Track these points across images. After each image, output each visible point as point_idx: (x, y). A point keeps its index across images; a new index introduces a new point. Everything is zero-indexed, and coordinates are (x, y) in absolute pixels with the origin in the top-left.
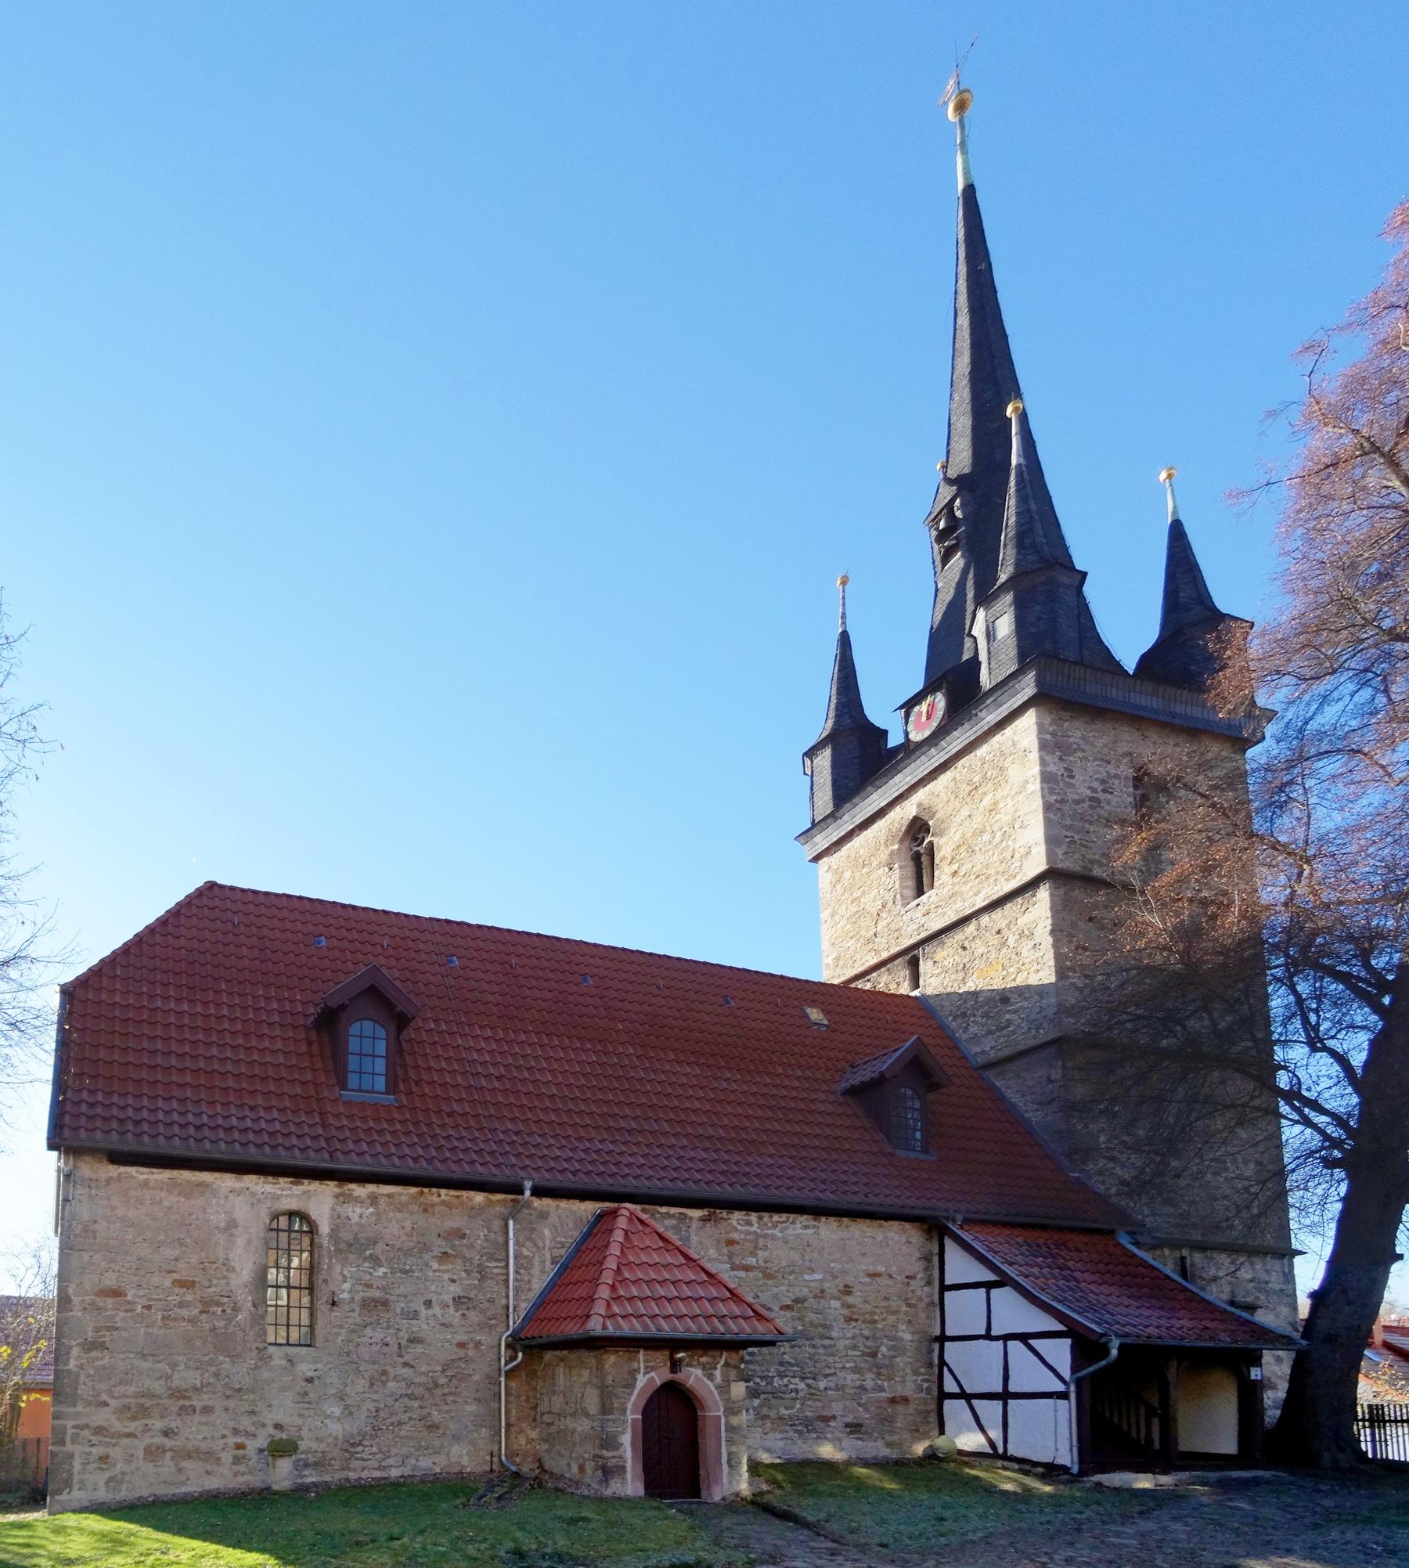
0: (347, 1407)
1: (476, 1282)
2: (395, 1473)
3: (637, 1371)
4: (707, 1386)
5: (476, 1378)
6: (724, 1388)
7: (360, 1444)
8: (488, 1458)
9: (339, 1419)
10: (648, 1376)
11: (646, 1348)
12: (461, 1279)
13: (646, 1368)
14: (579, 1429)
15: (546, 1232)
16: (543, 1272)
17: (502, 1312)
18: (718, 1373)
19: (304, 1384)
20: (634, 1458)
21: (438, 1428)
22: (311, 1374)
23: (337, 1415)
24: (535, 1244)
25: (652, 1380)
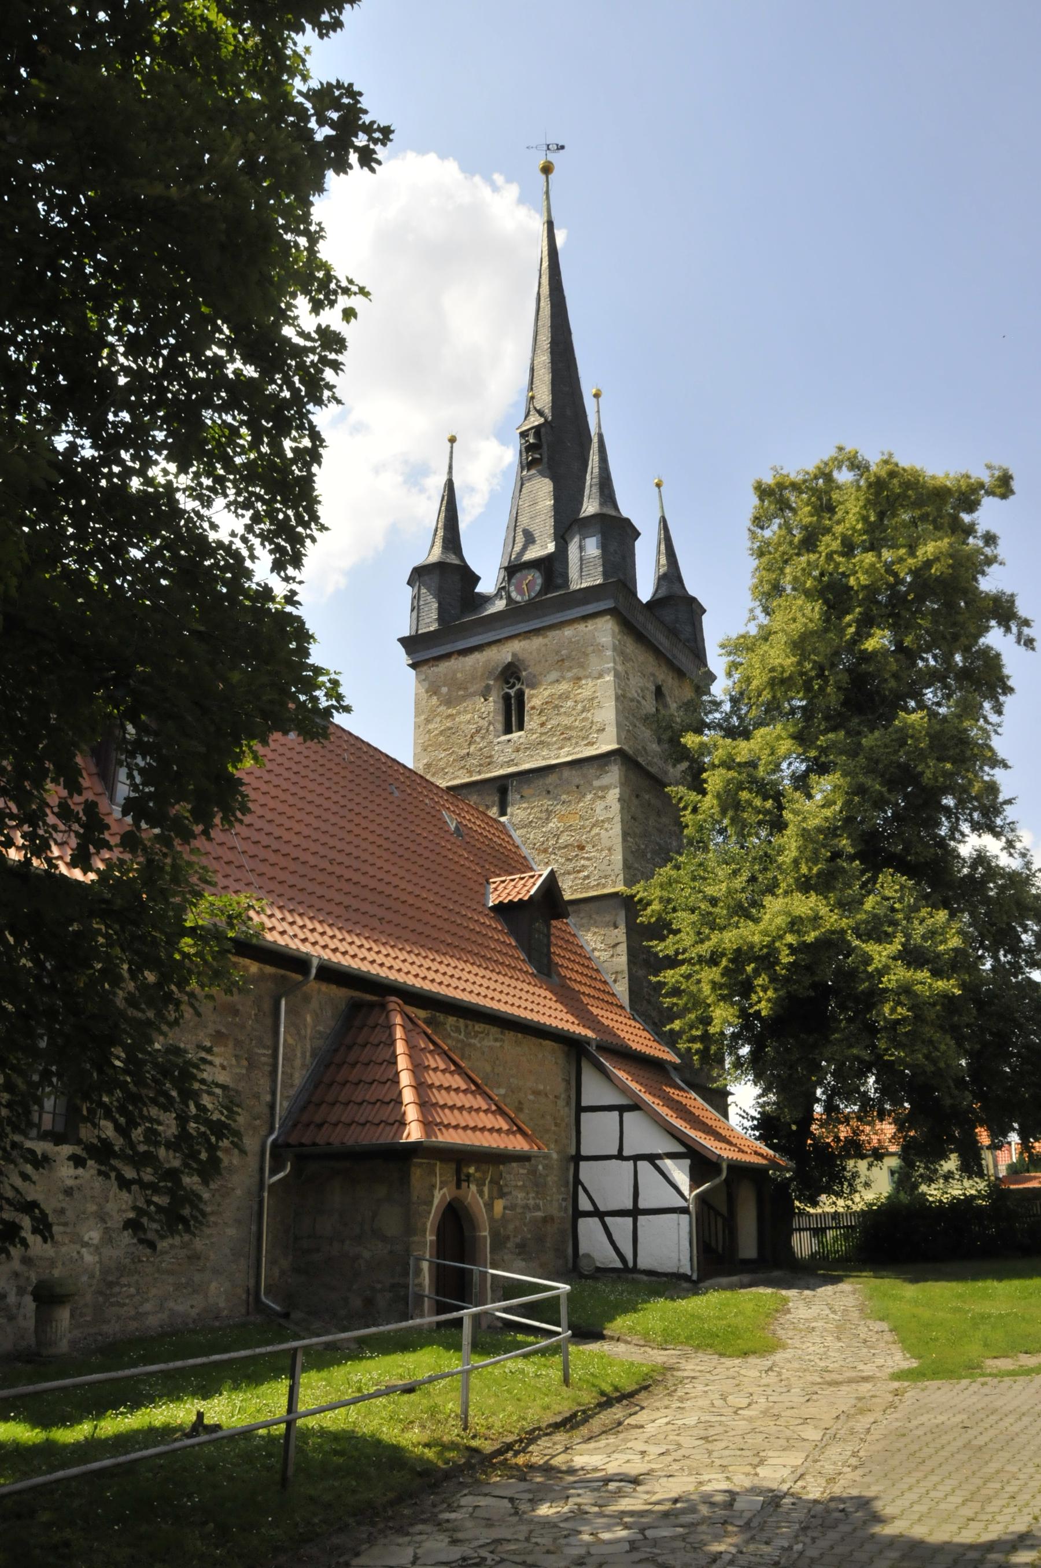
0: (107, 1230)
1: (244, 1071)
2: (153, 1321)
3: (434, 1186)
4: (478, 1203)
5: (238, 1192)
6: (489, 1206)
7: (118, 1283)
8: (244, 1297)
9: (97, 1248)
10: (442, 1192)
11: (442, 1161)
12: (231, 1066)
13: (441, 1182)
14: (367, 1254)
15: (309, 1019)
16: (303, 1065)
17: (266, 1110)
18: (486, 1189)
19: (61, 1197)
20: (430, 1280)
21: (199, 1258)
22: (70, 1182)
23: (96, 1242)
24: (299, 1033)
25: (444, 1194)
